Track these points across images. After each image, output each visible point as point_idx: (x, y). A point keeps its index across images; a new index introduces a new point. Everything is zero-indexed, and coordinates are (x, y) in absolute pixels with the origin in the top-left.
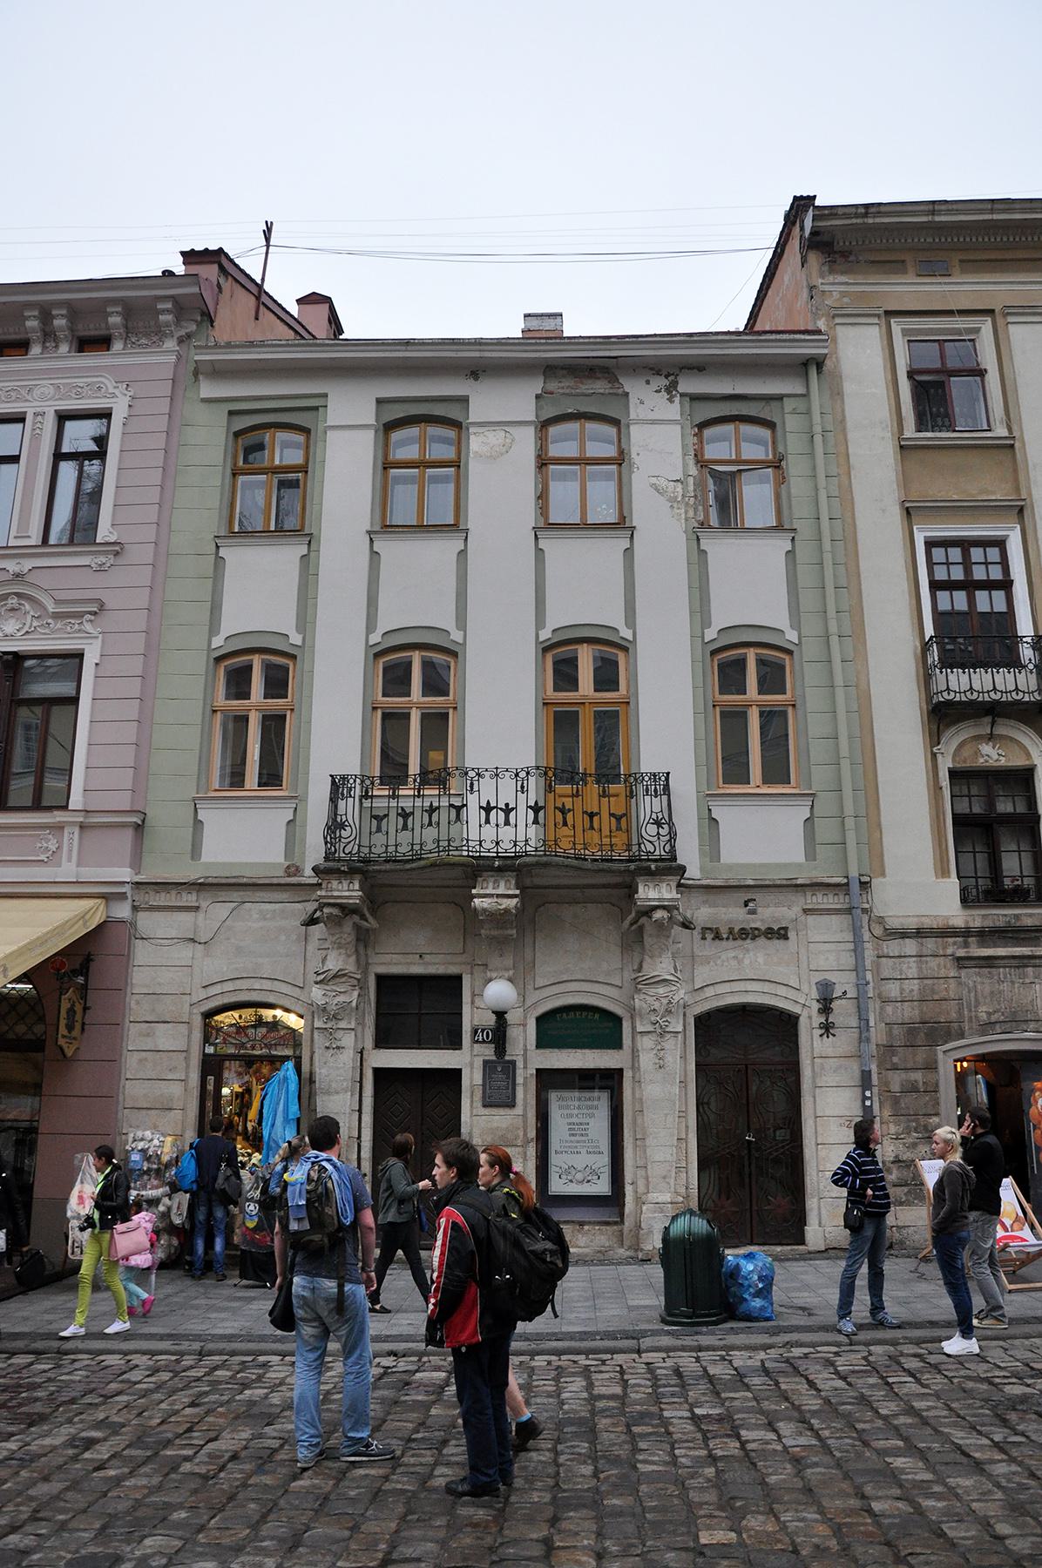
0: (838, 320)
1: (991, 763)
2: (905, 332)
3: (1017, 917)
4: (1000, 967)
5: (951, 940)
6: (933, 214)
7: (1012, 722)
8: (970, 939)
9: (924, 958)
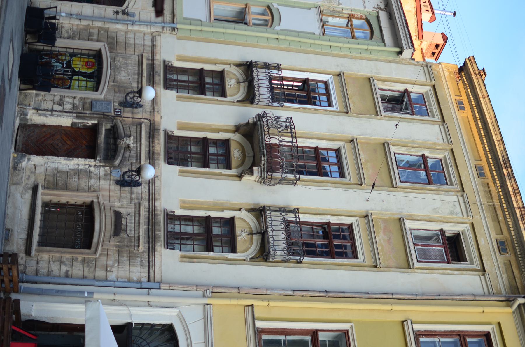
0: (426, 68)
1: (227, 83)
2: (427, 92)
3: (159, 75)
4: (138, 67)
5: (150, 55)
6: (483, 97)
7: (246, 92)
8: (150, 62)
9: (143, 46)
